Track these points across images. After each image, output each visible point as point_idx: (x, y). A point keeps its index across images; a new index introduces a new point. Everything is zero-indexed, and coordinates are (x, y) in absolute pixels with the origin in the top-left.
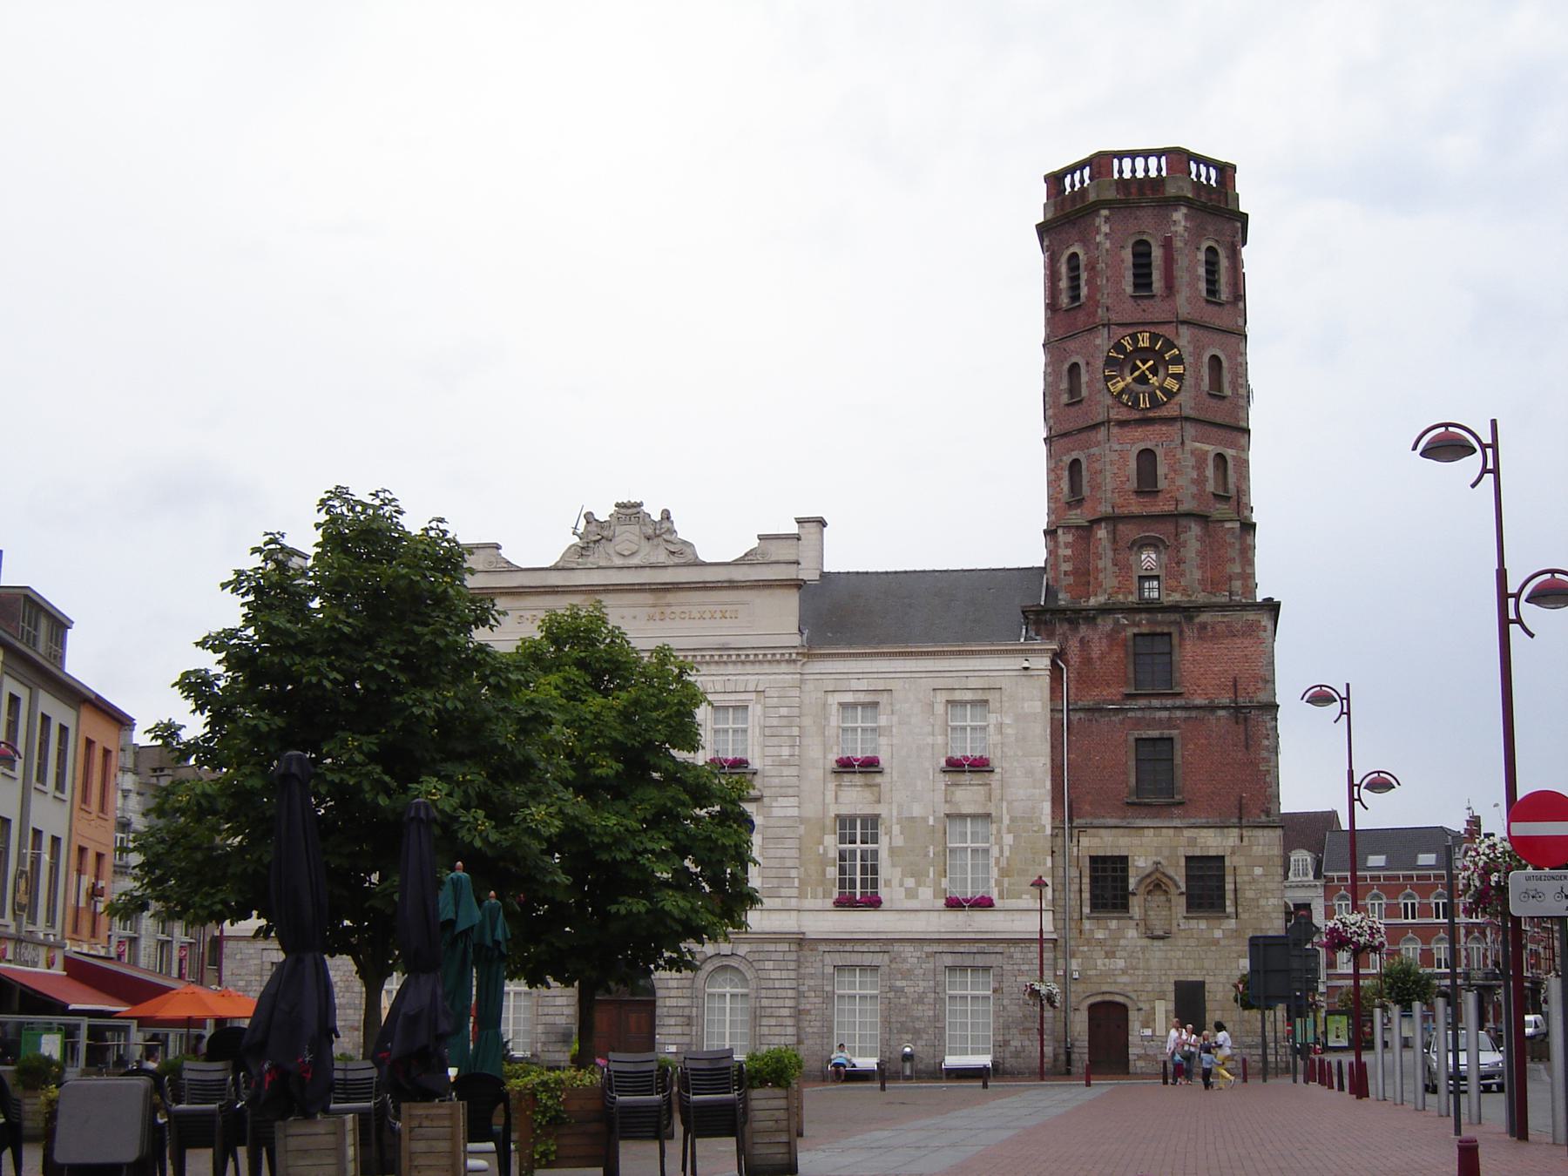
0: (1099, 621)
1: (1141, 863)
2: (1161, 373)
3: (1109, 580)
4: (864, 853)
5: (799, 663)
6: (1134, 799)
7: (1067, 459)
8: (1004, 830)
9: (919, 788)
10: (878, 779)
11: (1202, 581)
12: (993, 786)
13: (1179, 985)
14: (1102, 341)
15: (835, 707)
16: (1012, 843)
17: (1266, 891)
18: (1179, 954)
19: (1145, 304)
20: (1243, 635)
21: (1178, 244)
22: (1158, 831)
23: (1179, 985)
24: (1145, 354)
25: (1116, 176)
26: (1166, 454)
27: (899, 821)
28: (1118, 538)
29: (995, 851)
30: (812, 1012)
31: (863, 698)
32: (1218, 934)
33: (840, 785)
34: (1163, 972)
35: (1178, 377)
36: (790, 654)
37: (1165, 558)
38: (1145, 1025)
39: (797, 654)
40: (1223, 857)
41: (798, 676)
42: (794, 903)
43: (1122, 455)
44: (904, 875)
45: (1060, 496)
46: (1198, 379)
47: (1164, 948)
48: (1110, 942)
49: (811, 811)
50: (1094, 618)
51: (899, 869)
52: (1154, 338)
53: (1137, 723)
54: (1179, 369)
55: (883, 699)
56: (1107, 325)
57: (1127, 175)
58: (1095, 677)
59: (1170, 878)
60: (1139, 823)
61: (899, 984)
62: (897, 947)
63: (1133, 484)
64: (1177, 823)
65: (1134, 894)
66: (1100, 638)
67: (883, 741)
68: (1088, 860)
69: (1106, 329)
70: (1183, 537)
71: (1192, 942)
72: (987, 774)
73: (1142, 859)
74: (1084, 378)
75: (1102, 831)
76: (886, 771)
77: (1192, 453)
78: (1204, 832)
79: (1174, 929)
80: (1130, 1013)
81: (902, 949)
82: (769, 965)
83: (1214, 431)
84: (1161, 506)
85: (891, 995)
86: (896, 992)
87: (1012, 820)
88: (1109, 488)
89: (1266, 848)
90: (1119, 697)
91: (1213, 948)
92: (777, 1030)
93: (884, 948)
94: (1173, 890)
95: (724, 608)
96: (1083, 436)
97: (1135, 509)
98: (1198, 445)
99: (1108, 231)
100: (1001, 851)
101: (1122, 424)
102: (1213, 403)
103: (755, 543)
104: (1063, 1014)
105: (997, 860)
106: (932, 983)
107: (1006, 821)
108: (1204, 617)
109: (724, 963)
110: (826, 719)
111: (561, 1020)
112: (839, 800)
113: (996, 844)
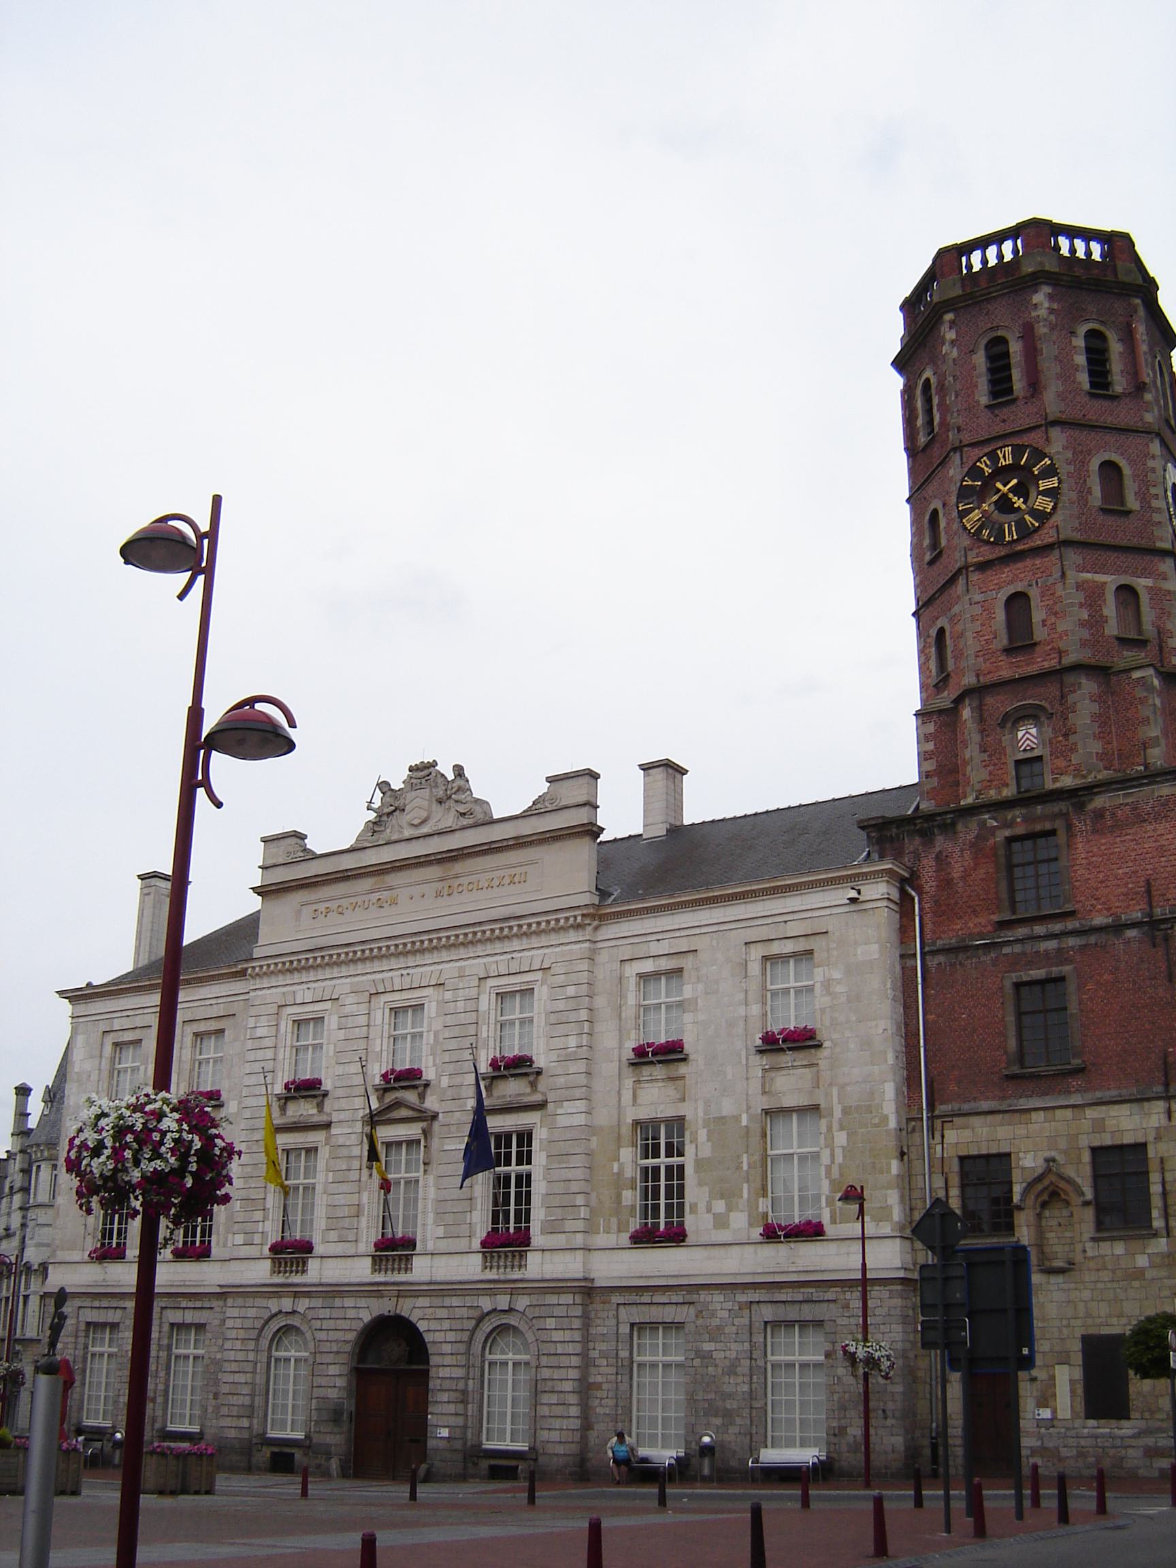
0: (960, 827)
1: (1028, 1162)
2: (1033, 493)
3: (976, 773)
4: (669, 1169)
5: (589, 929)
6: (1016, 1070)
7: (933, 632)
8: (835, 1126)
9: (729, 1076)
10: (683, 1069)
11: (1101, 756)
14: (955, 471)
15: (632, 983)
16: (845, 1144)
18: (1086, 1294)
19: (1005, 412)
20: (1156, 820)
21: (1042, 329)
22: (1049, 1114)
24: (1002, 473)
25: (965, 271)
26: (1043, 595)
27: (707, 1122)
28: (986, 714)
29: (825, 1158)
30: (605, 1386)
31: (665, 964)
32: (1142, 1261)
33: (639, 1082)
35: (1052, 493)
36: (575, 917)
37: (1049, 732)
39: (583, 915)
40: (1143, 1146)
41: (587, 945)
42: (579, 1240)
43: (986, 606)
44: (713, 1196)
45: (929, 681)
46: (1083, 493)
47: (1065, 1286)
49: (603, 1118)
50: (953, 824)
51: (706, 1189)
52: (1018, 451)
53: (1015, 962)
54: (1053, 482)
55: (687, 963)
56: (958, 449)
57: (977, 267)
58: (957, 903)
59: (1069, 1181)
60: (1024, 1103)
61: (707, 1347)
62: (704, 1296)
63: (1003, 641)
64: (1076, 1099)
65: (1019, 1208)
66: (962, 850)
67: (688, 1018)
68: (956, 1162)
69: (958, 454)
70: (1071, 699)
71: (1106, 1275)
72: (813, 1051)
73: (1030, 1156)
74: (943, 524)
76: (691, 1057)
77: (1079, 586)
78: (1115, 1110)
81: (709, 1298)
82: (551, 1323)
83: (1112, 556)
84: (1042, 662)
85: (697, 1362)
86: (703, 1358)
87: (846, 1111)
88: (971, 652)
90: (989, 928)
91: (1136, 1284)
92: (559, 1410)
93: (688, 1298)
94: (1075, 1200)
95: (513, 871)
96: (944, 598)
97: (1005, 674)
98: (1089, 576)
99: (954, 337)
100: (833, 1156)
101: (983, 566)
102: (1110, 520)
103: (544, 787)
104: (928, 1387)
105: (828, 1169)
106: (747, 1345)
107: (837, 1113)
108: (1099, 802)
109: (504, 1321)
110: (622, 996)
111: (333, 1394)
112: (639, 1101)
113: (826, 1147)
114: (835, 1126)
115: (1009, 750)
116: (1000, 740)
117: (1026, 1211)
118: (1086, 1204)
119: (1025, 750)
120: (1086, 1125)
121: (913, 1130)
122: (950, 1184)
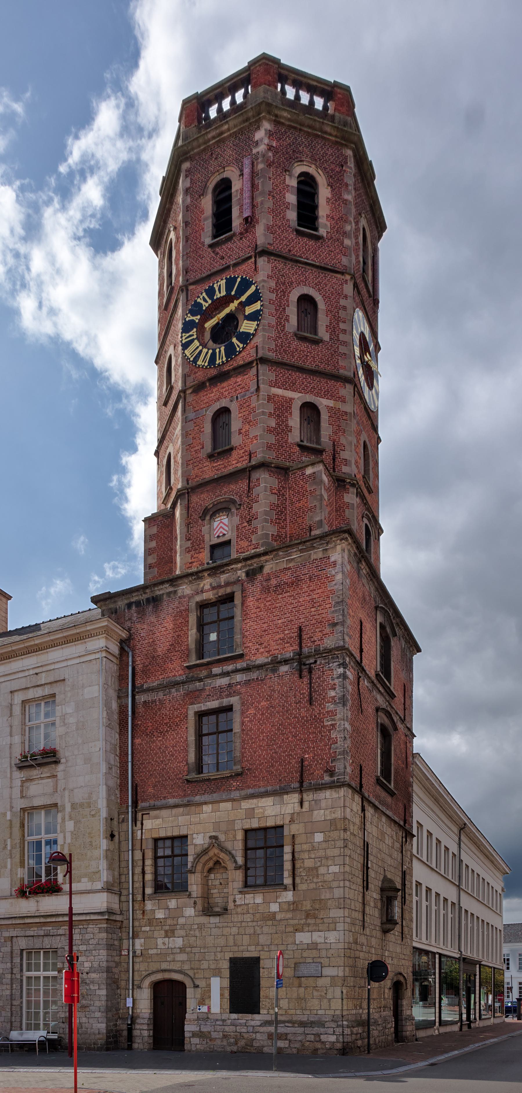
12: (59, 777)
13: (234, 962)
17: (327, 858)
23: (234, 962)
34: (219, 949)
38: (202, 1002)
48: (169, 922)
63: (208, 448)
64: (236, 794)
75: (164, 813)
79: (231, 906)
80: (188, 990)
87: (73, 806)
89: (327, 812)
107: (68, 808)
114: (67, 817)
115: (207, 537)
116: (201, 531)
117: (196, 874)
118: (237, 868)
119: (218, 537)
120: (241, 814)
121: (123, 821)
122: (146, 856)
